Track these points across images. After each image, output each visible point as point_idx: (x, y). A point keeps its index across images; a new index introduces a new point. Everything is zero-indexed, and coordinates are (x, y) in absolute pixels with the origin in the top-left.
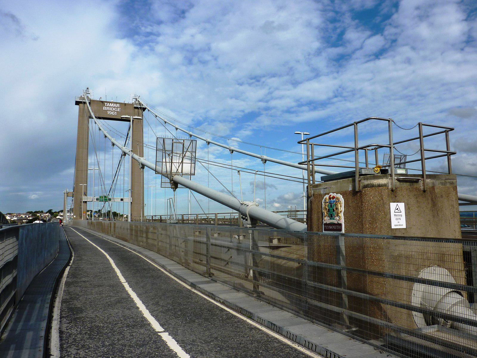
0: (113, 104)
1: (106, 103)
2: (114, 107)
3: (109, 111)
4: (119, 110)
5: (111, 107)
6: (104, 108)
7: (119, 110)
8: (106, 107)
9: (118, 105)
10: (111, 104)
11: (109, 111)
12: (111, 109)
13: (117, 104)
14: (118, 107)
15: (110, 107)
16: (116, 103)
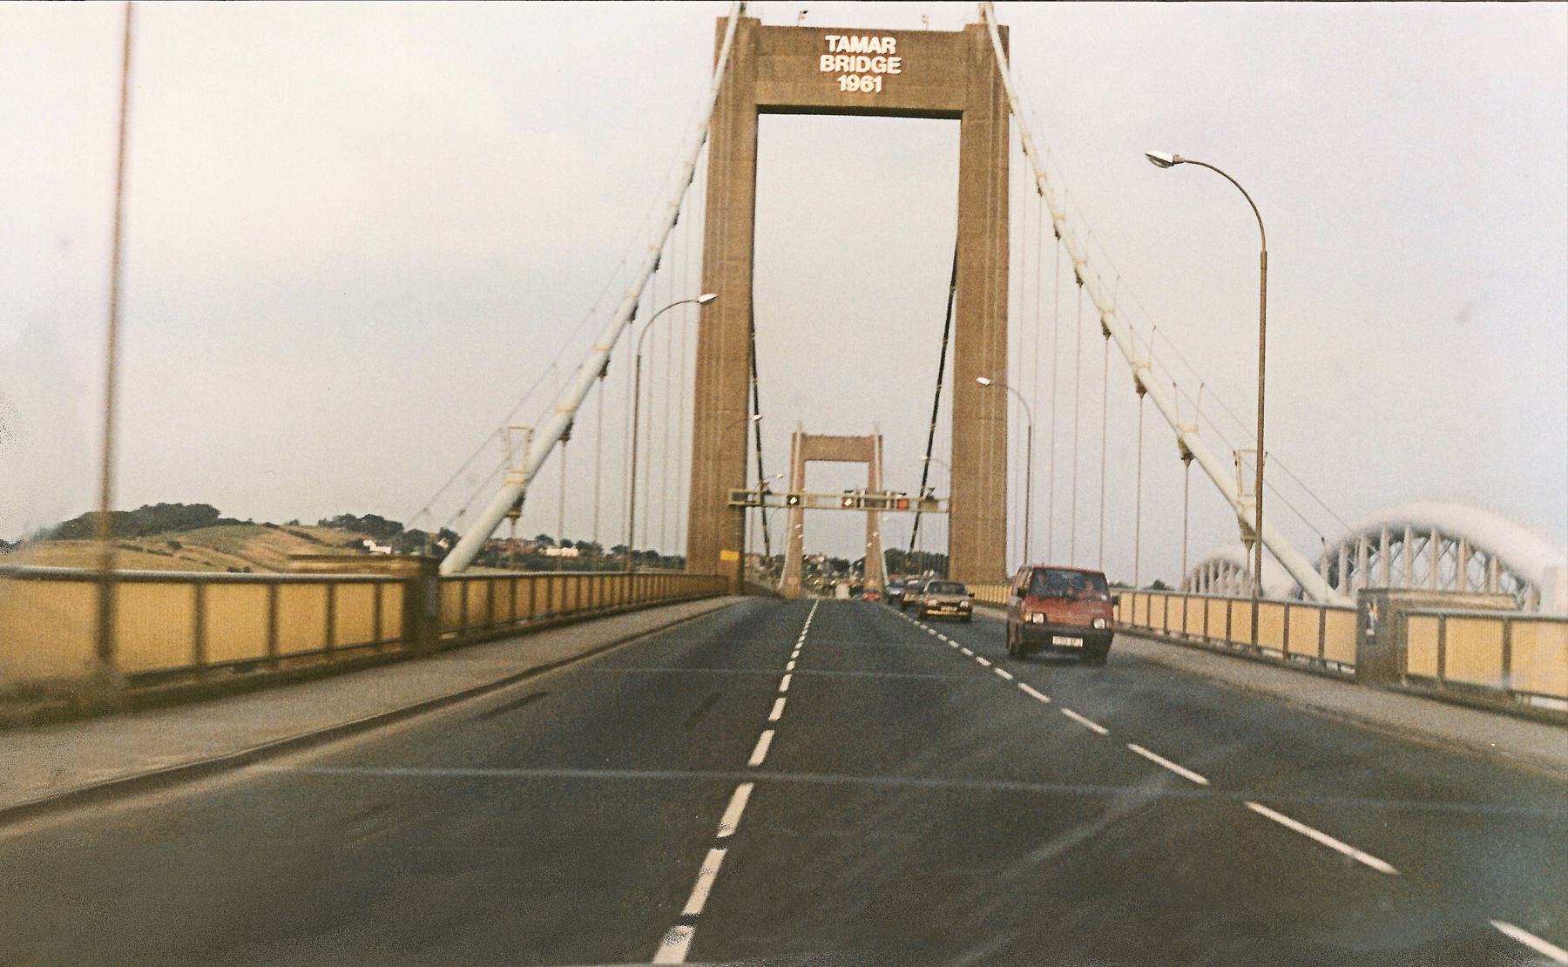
0: (865, 39)
1: (832, 39)
2: (873, 54)
3: (848, 74)
4: (892, 66)
5: (855, 54)
6: (826, 63)
7: (891, 65)
8: (834, 54)
9: (890, 44)
10: (854, 39)
11: (848, 74)
12: (854, 64)
13: (885, 40)
14: (887, 55)
15: (850, 55)
16: (880, 34)
